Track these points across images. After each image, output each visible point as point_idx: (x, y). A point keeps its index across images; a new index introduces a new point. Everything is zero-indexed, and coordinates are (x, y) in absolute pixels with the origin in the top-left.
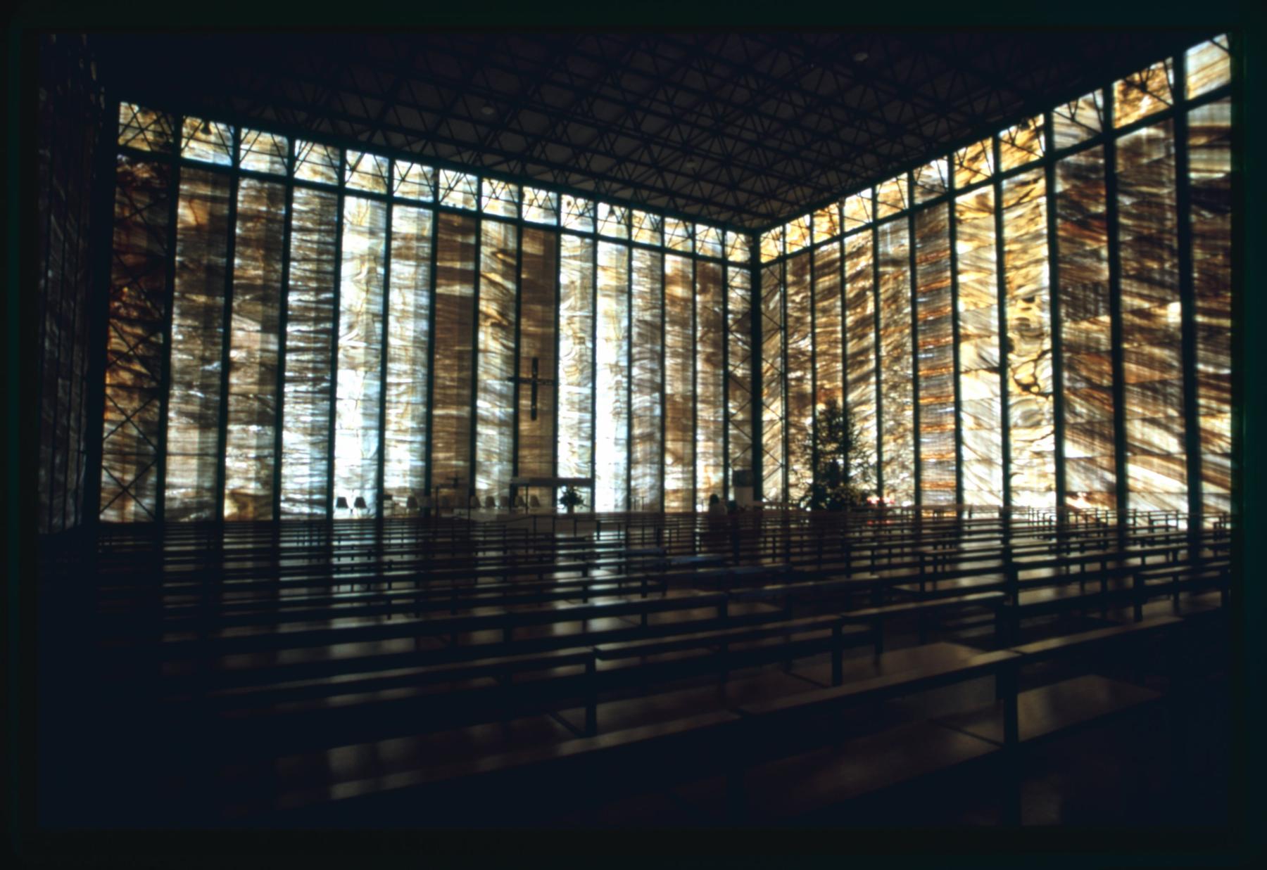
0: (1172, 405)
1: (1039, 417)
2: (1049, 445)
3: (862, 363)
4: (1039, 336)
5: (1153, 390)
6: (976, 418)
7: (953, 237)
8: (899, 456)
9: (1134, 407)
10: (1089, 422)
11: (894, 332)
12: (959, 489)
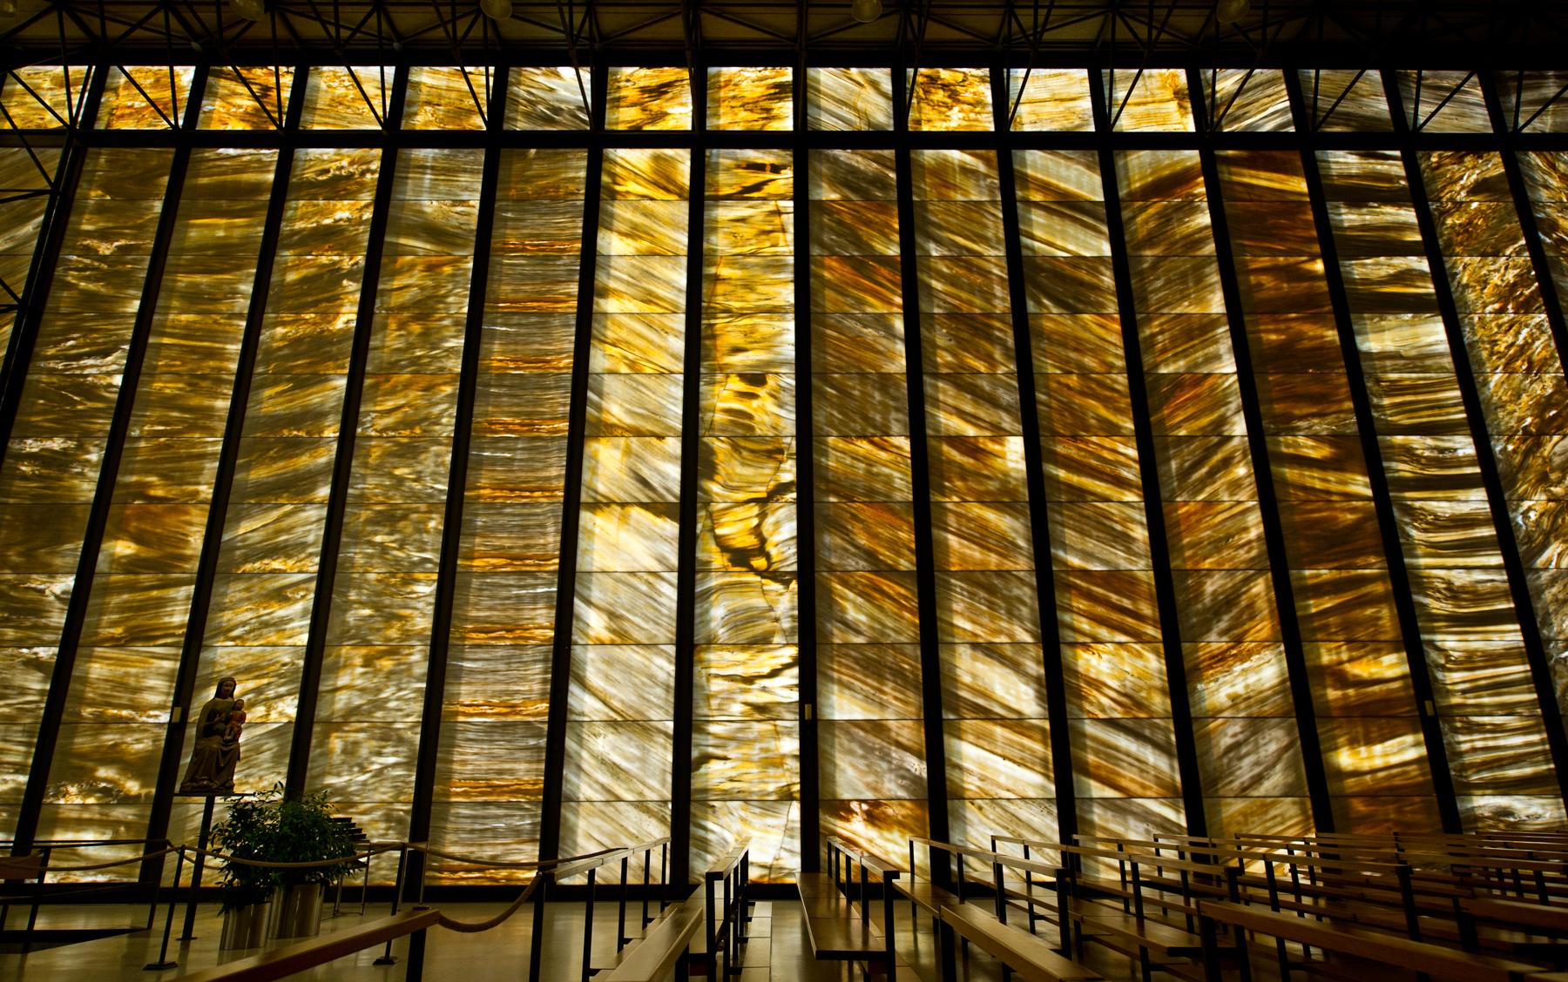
0: (1020, 619)
1: (767, 625)
2: (785, 689)
3: (294, 447)
4: (774, 454)
5: (985, 583)
6: (612, 615)
7: (594, 219)
8: (380, 705)
9: (962, 619)
10: (873, 643)
11: (407, 386)
12: (553, 801)
